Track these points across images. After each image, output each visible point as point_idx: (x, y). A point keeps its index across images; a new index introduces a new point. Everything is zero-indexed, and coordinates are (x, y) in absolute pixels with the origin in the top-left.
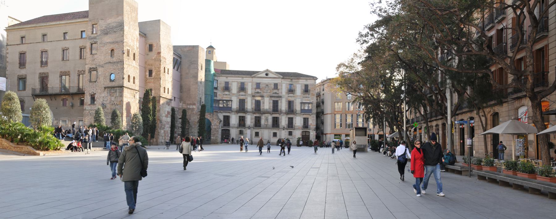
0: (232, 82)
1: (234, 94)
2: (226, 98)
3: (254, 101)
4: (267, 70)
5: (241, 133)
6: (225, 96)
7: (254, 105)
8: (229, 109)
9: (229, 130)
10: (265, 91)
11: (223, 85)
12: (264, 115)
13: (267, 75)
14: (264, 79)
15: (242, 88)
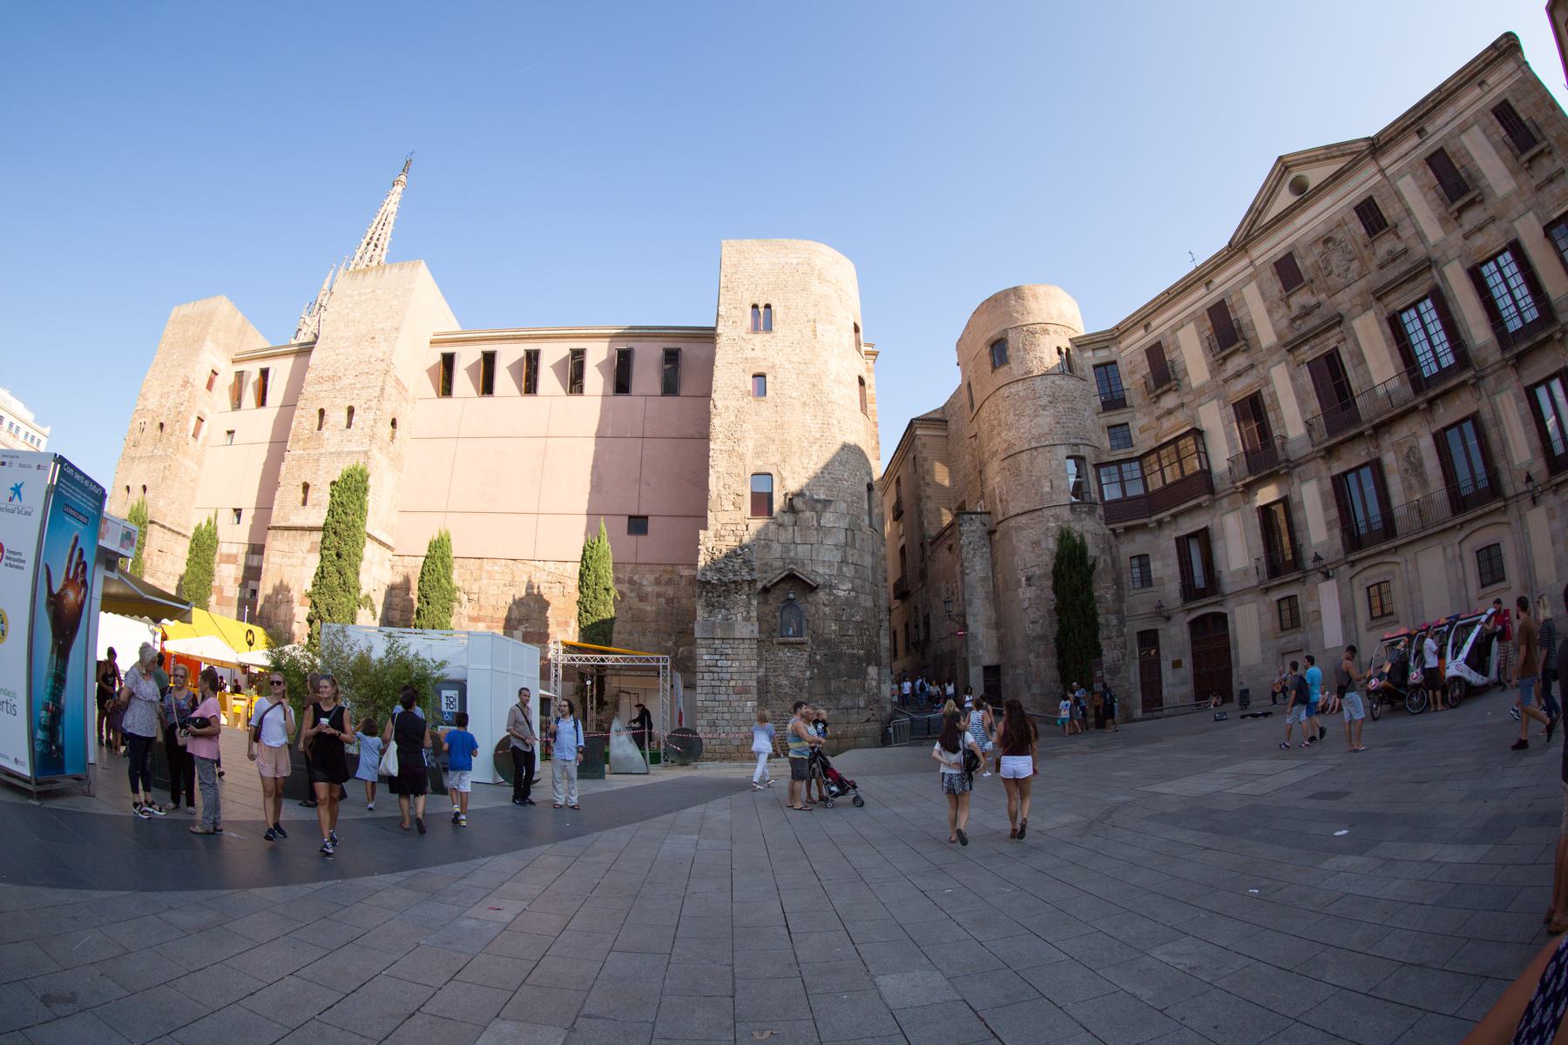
0: (1175, 329)
1: (1201, 391)
2: (1173, 426)
3: (1306, 377)
4: (1284, 165)
5: (1290, 617)
6: (1167, 423)
7: (1314, 404)
8: (1203, 483)
9: (1223, 617)
10: (1333, 280)
11: (1144, 369)
12: (1387, 441)
13: (1299, 187)
14: (1300, 220)
15: (1225, 331)
